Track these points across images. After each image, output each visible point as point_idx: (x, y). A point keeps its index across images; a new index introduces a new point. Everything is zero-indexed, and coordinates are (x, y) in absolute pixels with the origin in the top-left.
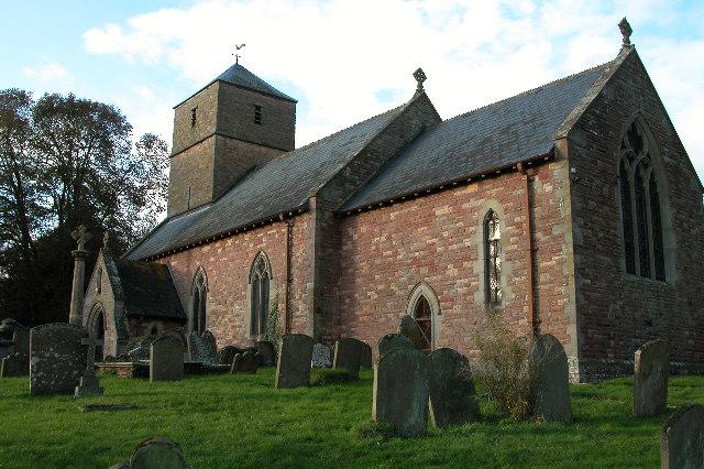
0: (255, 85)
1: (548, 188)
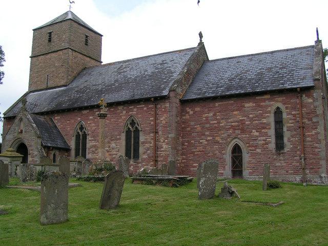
0: (82, 23)
1: (310, 100)
